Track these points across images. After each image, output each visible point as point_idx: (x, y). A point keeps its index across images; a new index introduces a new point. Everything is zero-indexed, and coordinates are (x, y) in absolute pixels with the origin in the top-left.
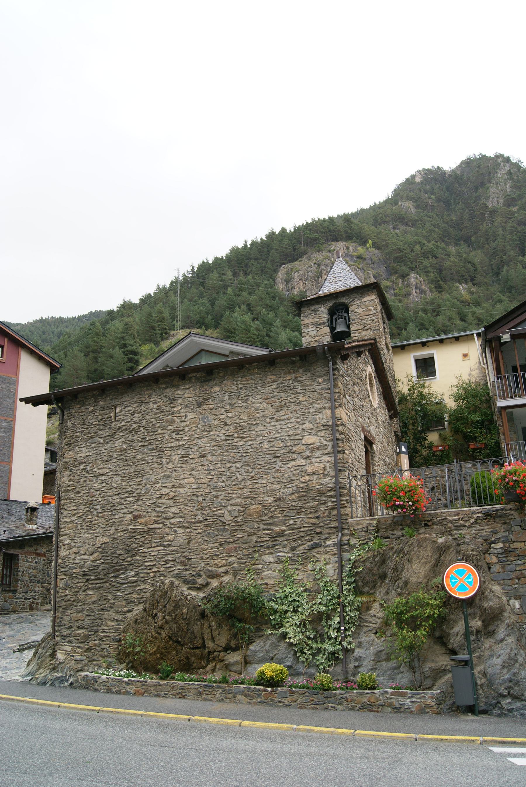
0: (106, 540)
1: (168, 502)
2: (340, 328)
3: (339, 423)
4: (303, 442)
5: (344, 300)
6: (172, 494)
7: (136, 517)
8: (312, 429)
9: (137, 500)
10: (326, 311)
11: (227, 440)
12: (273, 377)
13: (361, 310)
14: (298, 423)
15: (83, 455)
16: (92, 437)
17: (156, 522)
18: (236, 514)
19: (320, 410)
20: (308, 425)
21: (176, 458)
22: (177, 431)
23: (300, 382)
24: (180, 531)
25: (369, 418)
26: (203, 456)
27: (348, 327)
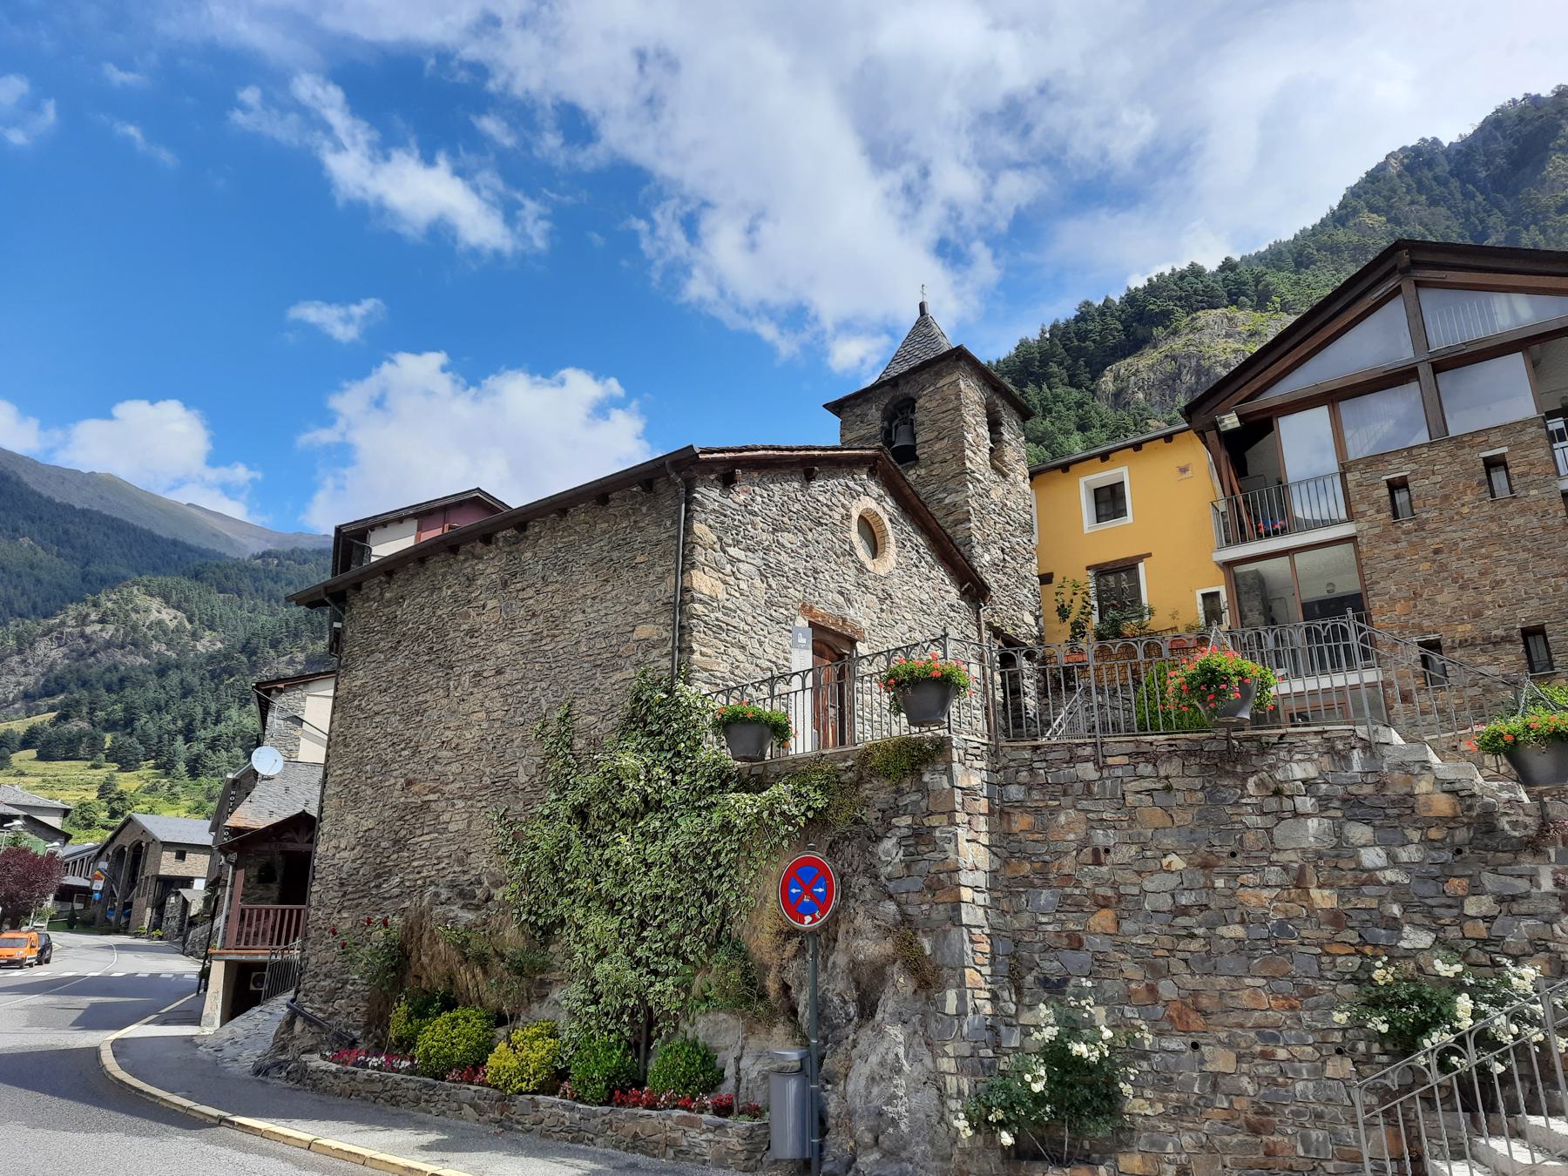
0: (370, 824)
1: (450, 754)
2: (901, 441)
3: (687, 597)
4: (635, 637)
5: (906, 389)
6: (456, 740)
7: (409, 783)
8: (647, 613)
9: (414, 755)
10: (879, 414)
11: (533, 641)
12: (605, 526)
13: (935, 404)
14: (629, 602)
15: (358, 683)
16: (373, 652)
17: (432, 791)
18: (534, 770)
19: (661, 579)
20: (644, 606)
21: (466, 679)
22: (471, 633)
23: (641, 530)
24: (460, 804)
25: (842, 594)
26: (499, 672)
27: (914, 436)
